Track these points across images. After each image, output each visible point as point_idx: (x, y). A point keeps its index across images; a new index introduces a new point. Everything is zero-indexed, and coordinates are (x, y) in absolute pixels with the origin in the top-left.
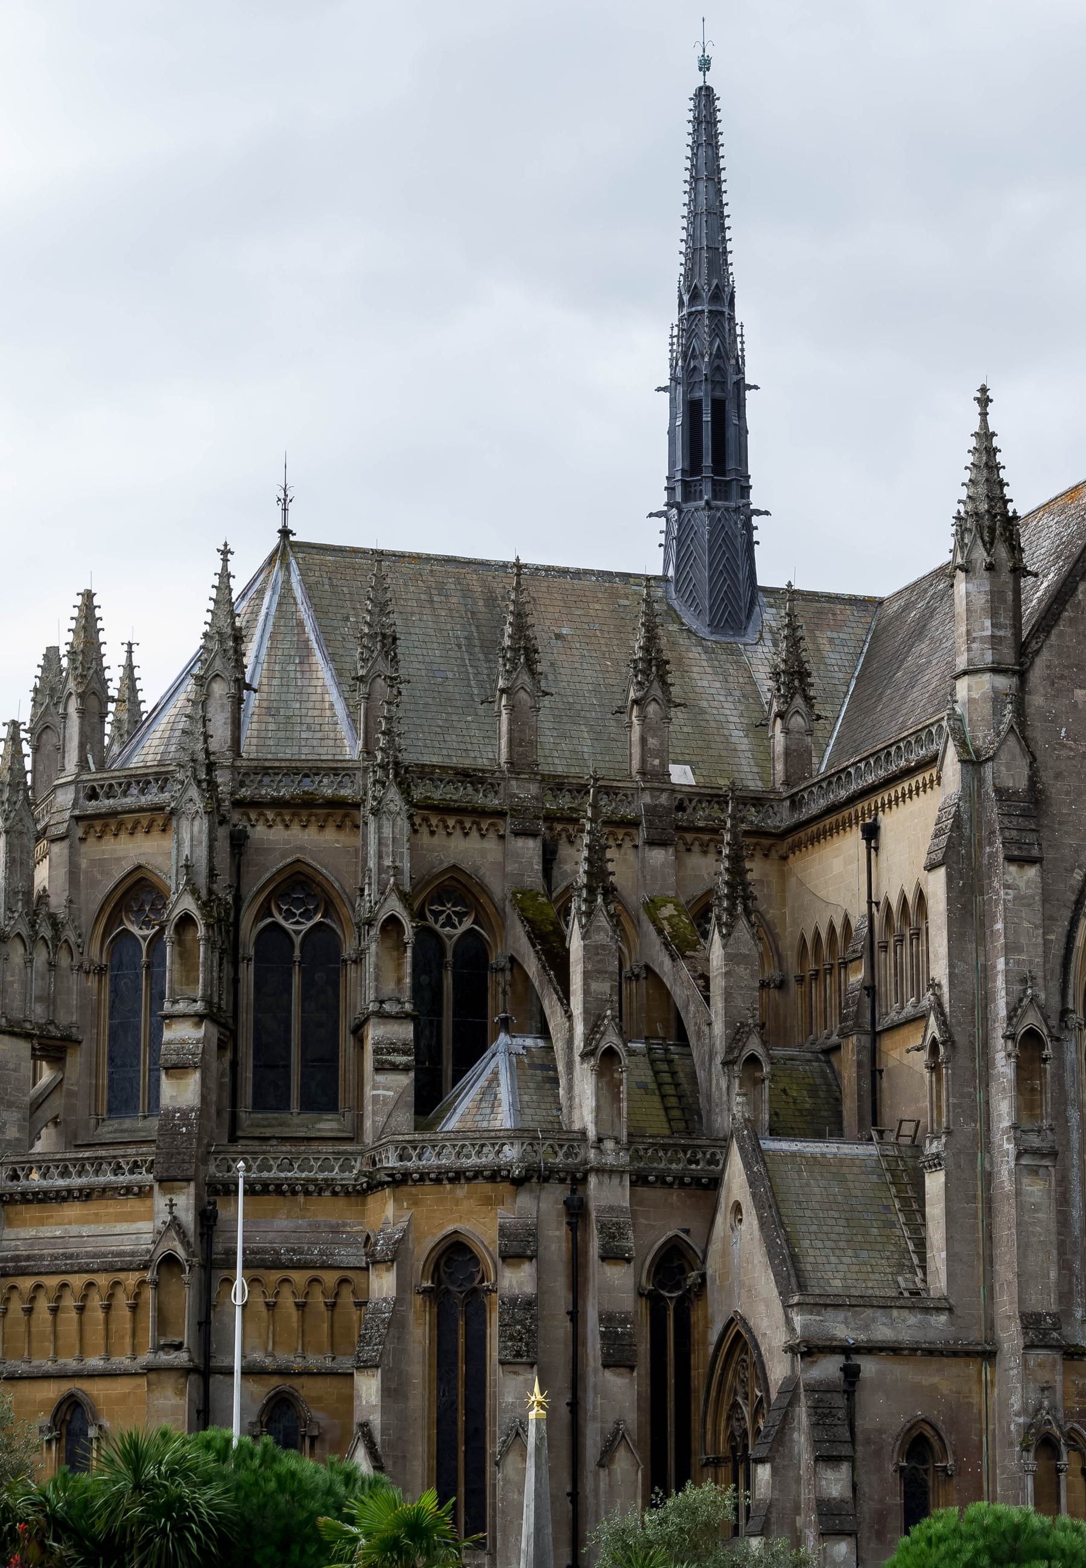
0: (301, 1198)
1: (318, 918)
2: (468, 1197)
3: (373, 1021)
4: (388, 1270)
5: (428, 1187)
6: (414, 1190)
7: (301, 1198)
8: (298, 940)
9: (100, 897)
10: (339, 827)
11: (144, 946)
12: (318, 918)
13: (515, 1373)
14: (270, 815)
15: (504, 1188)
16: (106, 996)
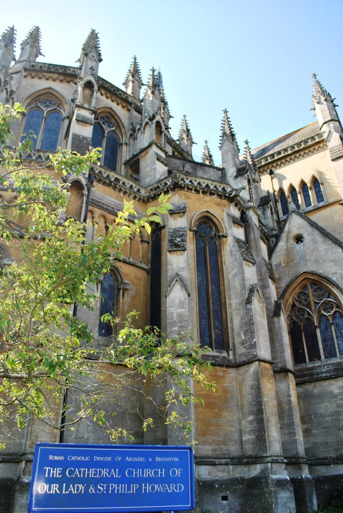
0: (121, 194)
1: (113, 129)
2: (211, 201)
3: (154, 146)
4: (181, 216)
5: (193, 194)
6: (187, 193)
7: (121, 194)
8: (106, 132)
9: (29, 93)
10: (123, 107)
11: (45, 113)
12: (113, 129)
13: (248, 266)
14: (103, 92)
15: (225, 202)
16: (24, 122)
